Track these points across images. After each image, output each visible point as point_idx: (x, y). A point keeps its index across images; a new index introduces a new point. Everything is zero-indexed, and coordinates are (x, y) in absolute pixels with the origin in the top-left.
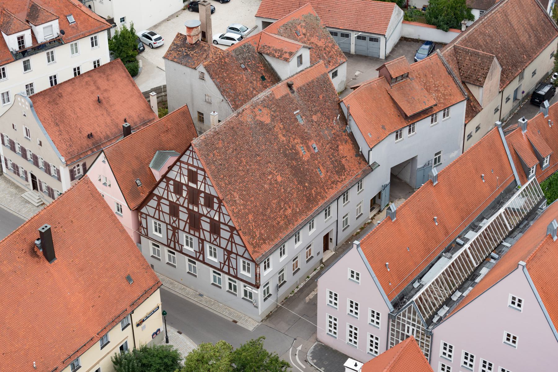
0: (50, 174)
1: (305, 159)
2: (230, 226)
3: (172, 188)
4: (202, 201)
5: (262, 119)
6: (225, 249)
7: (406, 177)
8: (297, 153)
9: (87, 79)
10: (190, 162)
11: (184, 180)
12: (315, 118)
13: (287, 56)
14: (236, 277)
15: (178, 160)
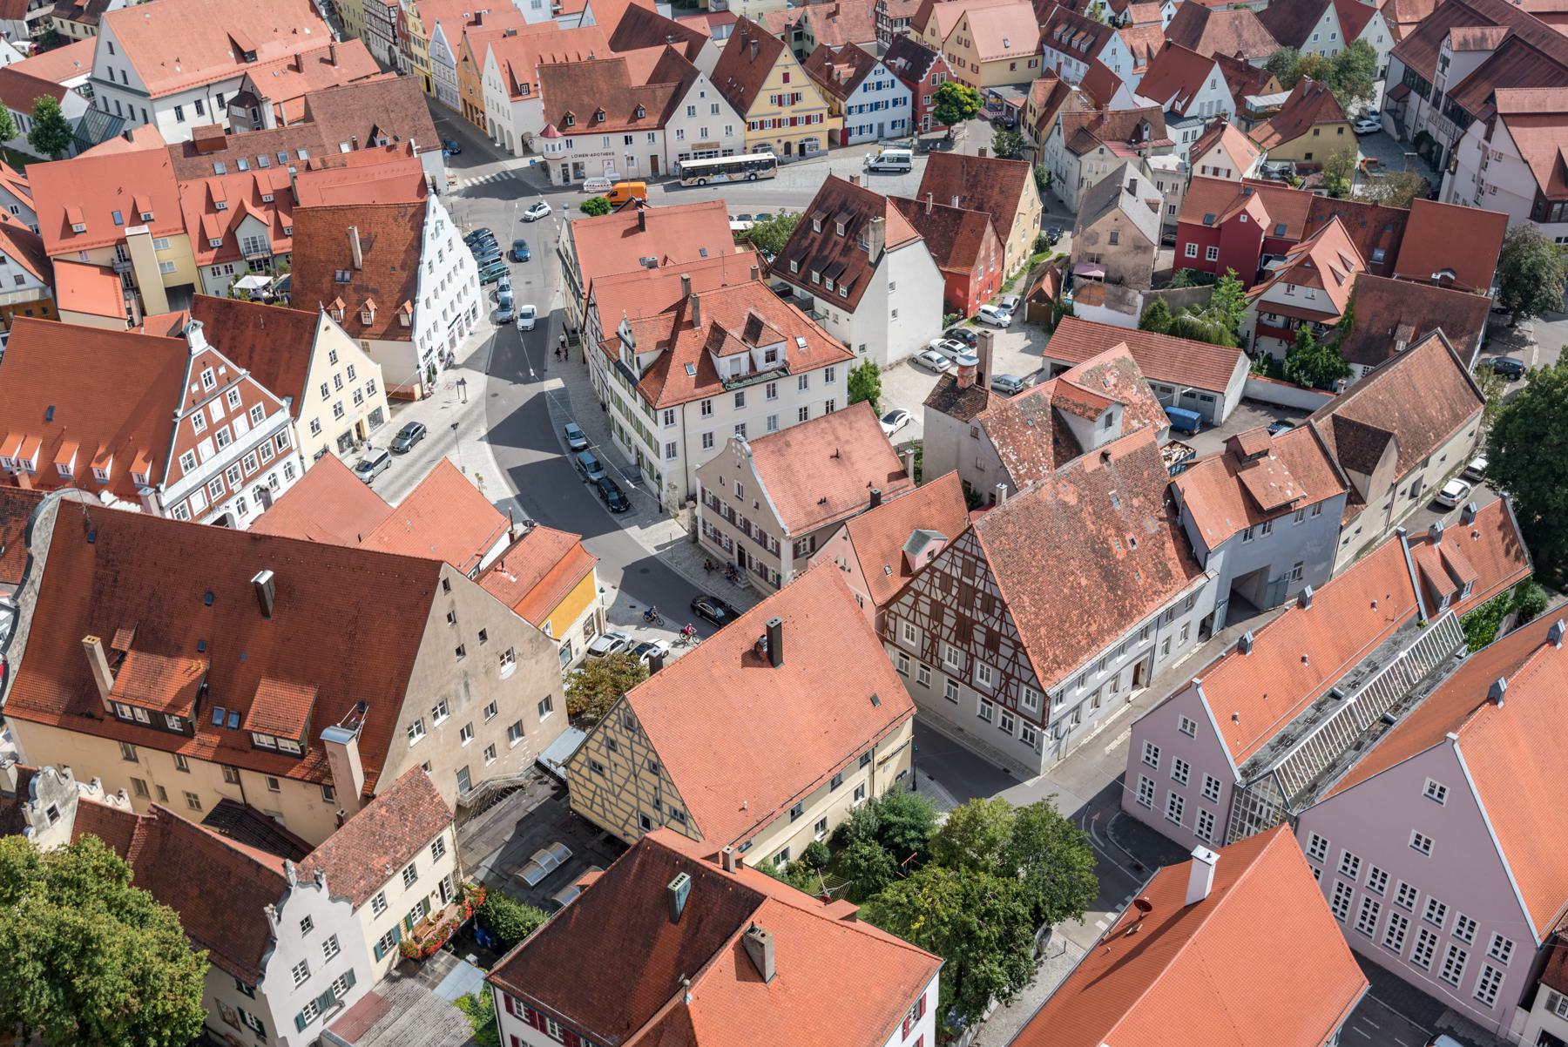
0: (765, 547)
1: (1120, 557)
2: (1014, 642)
3: (937, 582)
4: (978, 603)
5: (1066, 499)
6: (1003, 672)
7: (1249, 592)
8: (1109, 549)
9: (824, 425)
10: (968, 549)
11: (956, 573)
12: (1136, 502)
13: (1091, 413)
14: (1014, 710)
15: (951, 545)
